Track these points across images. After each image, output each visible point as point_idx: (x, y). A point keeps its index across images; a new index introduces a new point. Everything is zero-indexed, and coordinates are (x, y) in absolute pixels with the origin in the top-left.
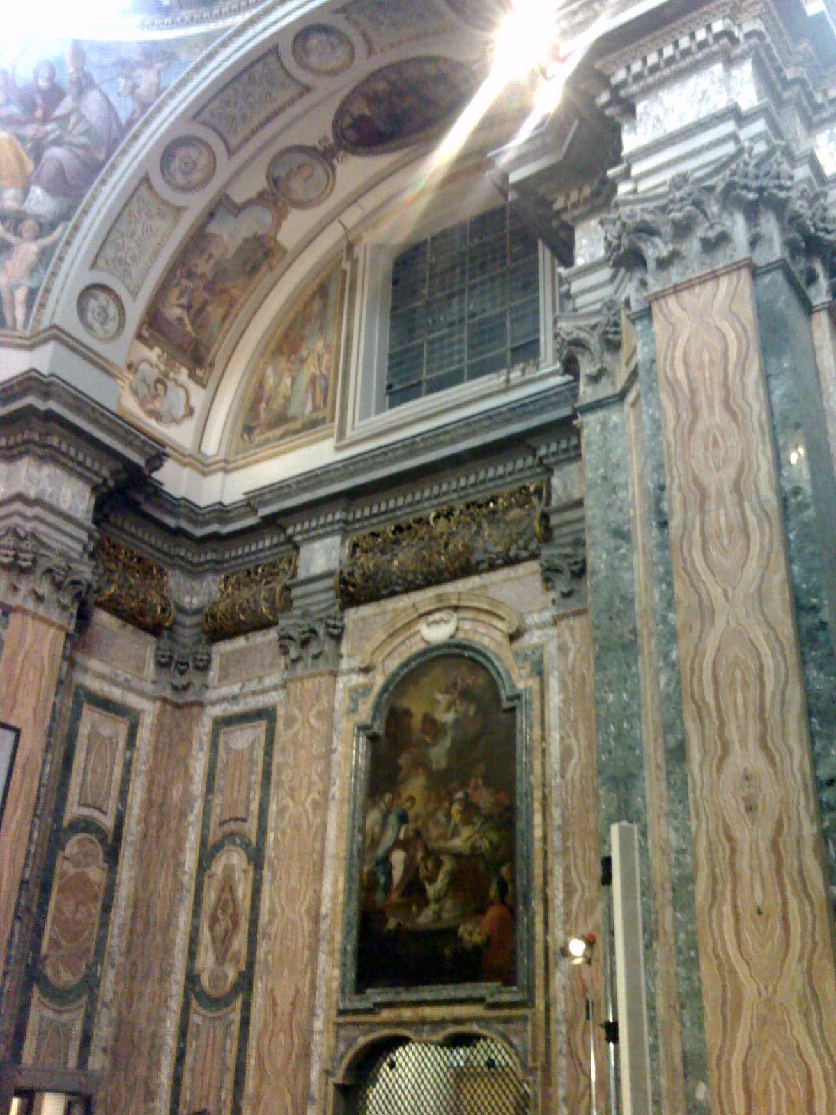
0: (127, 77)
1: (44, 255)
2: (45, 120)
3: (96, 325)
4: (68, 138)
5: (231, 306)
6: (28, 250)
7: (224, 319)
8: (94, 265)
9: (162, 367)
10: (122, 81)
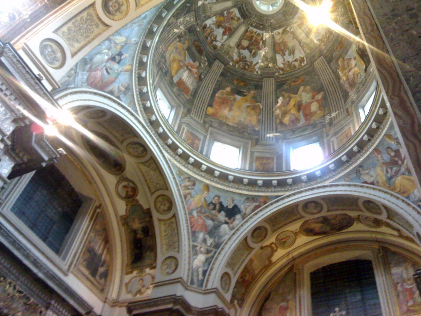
2: (403, 162)
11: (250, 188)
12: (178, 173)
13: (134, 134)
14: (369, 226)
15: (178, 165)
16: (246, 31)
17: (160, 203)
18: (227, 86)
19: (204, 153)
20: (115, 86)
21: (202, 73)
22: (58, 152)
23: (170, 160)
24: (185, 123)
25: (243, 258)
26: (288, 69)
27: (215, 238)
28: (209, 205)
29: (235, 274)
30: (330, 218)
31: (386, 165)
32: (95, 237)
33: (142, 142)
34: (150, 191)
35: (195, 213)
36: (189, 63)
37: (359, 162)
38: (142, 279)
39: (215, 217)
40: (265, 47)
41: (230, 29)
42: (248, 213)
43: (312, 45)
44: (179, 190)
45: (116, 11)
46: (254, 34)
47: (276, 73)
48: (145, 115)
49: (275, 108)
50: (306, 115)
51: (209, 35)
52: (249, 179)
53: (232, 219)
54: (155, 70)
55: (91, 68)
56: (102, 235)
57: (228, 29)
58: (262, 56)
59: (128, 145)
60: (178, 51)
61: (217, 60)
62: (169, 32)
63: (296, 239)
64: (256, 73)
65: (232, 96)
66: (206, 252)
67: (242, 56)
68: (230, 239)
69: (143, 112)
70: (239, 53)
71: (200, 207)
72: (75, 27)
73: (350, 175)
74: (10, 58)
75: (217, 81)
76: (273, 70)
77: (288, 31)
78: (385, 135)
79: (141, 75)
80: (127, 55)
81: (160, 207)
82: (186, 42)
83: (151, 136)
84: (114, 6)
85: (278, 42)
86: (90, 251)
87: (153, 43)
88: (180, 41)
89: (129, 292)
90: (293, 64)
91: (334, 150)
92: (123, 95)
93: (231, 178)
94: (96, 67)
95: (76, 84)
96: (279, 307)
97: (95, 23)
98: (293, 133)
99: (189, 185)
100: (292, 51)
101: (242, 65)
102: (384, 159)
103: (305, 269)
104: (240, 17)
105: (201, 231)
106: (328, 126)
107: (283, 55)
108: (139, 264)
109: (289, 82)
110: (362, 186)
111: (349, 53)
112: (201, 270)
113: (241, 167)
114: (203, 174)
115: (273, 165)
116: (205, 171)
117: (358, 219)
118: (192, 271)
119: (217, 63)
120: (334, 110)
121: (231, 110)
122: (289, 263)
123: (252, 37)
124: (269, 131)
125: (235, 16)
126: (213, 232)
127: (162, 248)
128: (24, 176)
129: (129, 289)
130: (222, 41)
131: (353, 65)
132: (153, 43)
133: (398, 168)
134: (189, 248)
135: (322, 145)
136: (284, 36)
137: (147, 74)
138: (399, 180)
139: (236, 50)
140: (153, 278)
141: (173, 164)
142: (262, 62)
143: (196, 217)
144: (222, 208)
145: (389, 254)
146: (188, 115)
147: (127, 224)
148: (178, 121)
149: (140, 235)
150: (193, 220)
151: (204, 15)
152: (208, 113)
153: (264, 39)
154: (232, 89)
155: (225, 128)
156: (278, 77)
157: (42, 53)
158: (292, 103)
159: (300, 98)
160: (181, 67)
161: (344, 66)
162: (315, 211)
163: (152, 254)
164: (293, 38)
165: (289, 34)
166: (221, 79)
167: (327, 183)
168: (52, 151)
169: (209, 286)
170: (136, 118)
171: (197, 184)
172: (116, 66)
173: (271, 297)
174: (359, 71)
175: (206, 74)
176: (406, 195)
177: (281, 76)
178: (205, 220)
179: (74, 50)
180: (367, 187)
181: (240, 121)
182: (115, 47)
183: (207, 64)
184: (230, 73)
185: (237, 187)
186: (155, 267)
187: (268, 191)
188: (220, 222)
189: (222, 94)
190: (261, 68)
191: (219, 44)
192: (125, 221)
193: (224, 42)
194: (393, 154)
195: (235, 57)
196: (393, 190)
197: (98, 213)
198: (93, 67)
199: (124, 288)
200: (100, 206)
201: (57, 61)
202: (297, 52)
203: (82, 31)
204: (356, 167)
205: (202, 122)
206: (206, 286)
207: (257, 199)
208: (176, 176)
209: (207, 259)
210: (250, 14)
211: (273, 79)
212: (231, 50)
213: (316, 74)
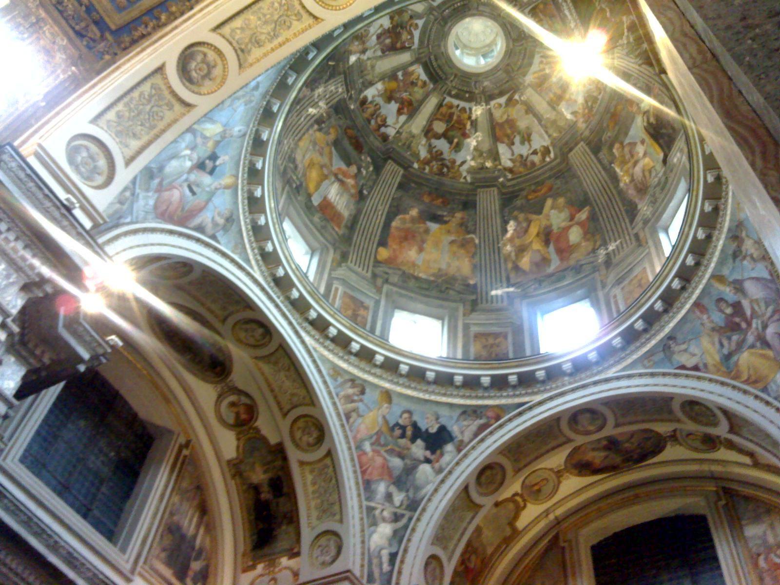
0: (744, 258)
2: (749, 324)
10: (745, 262)
11: (468, 392)
12: (331, 372)
13: (247, 304)
14: (696, 450)
15: (331, 357)
16: (440, 106)
17: (300, 431)
18: (413, 207)
19: (378, 332)
20: (206, 217)
21: (363, 185)
22: (107, 342)
23: (315, 349)
24: (337, 279)
25: (464, 525)
26: (521, 169)
27: (407, 491)
28: (392, 429)
29: (450, 559)
30: (620, 439)
31: (718, 331)
32: (181, 504)
33: (259, 318)
34: (281, 409)
35: (367, 447)
36: (340, 169)
37: (667, 330)
38: (274, 579)
39: (405, 452)
40: (476, 131)
41: (410, 103)
42: (466, 439)
43: (562, 123)
44: (334, 404)
45: (204, 77)
46: (453, 110)
47: (499, 177)
48: (264, 268)
49: (501, 242)
50: (560, 252)
51: (372, 115)
52: (465, 376)
53: (438, 452)
54: (279, 185)
55: (160, 184)
56: (194, 498)
57: (406, 103)
58: (472, 148)
59: (235, 324)
60: (317, 148)
61: (390, 161)
62: (299, 114)
63: (559, 483)
64: (462, 180)
65: (422, 225)
66: (393, 517)
67: (434, 150)
68: (436, 490)
69: (261, 263)
70: (430, 145)
71: (377, 433)
72: (130, 110)
73: (652, 356)
74: (13, 172)
75: (393, 199)
77: (517, 101)
78: (713, 276)
79: (253, 193)
80: (226, 158)
81: (300, 439)
82: (332, 131)
83: (277, 306)
84: (200, 69)
85: (500, 121)
86: (172, 530)
87: (272, 135)
88: (320, 130)
90: (529, 159)
91: (618, 311)
92: (221, 232)
93: (430, 375)
94: (170, 183)
95: (135, 214)
97: (166, 101)
98: (540, 285)
99: (354, 394)
100: (526, 136)
101: (435, 167)
102: (712, 322)
103: (582, 540)
104: (428, 81)
105: (382, 479)
106: (603, 268)
108: (266, 550)
109: (524, 193)
110: (676, 375)
111: (632, 132)
112: (385, 554)
113: (448, 353)
114: (378, 371)
115: (507, 348)
116: (382, 366)
117: (674, 437)
118: (369, 557)
119: (390, 166)
120: (612, 238)
121: (421, 250)
122: (551, 529)
124: (494, 284)
125: (418, 79)
126: (403, 480)
127: (309, 516)
128: (44, 392)
130: (398, 126)
131: (641, 155)
132: (272, 135)
133: (742, 337)
134: (361, 513)
135: (596, 304)
136: (510, 109)
137: (266, 191)
138: (745, 358)
139: (424, 141)
140: (296, 574)
141: (322, 356)
142: (473, 159)
143: (370, 454)
144: (417, 433)
145: (738, 501)
146: (343, 264)
148: (326, 276)
151: (361, 81)
152: (379, 258)
153: (474, 117)
155: (412, 283)
156: (503, 185)
157: (71, 161)
158: (534, 230)
159: (548, 220)
160: (326, 177)
161: (623, 156)
162: (592, 428)
163: (291, 529)
165: (519, 106)
166: (399, 194)
167: (610, 373)
168: (97, 342)
170: (249, 274)
171: (368, 390)
172: (207, 180)
174: (652, 164)
175: (372, 188)
176: (761, 385)
177: (509, 184)
178: (388, 457)
179: (129, 153)
180: (687, 376)
181: (440, 270)
182: (204, 144)
183: (371, 169)
184: (416, 183)
185: (443, 392)
186: (298, 554)
187: (501, 396)
188: (415, 460)
189: (404, 221)
190: (470, 171)
191: (391, 132)
192: (236, 469)
193: (401, 127)
194: (729, 311)
195: (423, 154)
196: (736, 377)
197: (185, 457)
198: (165, 183)
200: (187, 445)
201: (99, 174)
202: (535, 137)
203: (142, 117)
204: (661, 340)
205: (369, 275)
208: (328, 378)
209: (395, 532)
210: (445, 73)
211: (495, 189)
213: (575, 176)
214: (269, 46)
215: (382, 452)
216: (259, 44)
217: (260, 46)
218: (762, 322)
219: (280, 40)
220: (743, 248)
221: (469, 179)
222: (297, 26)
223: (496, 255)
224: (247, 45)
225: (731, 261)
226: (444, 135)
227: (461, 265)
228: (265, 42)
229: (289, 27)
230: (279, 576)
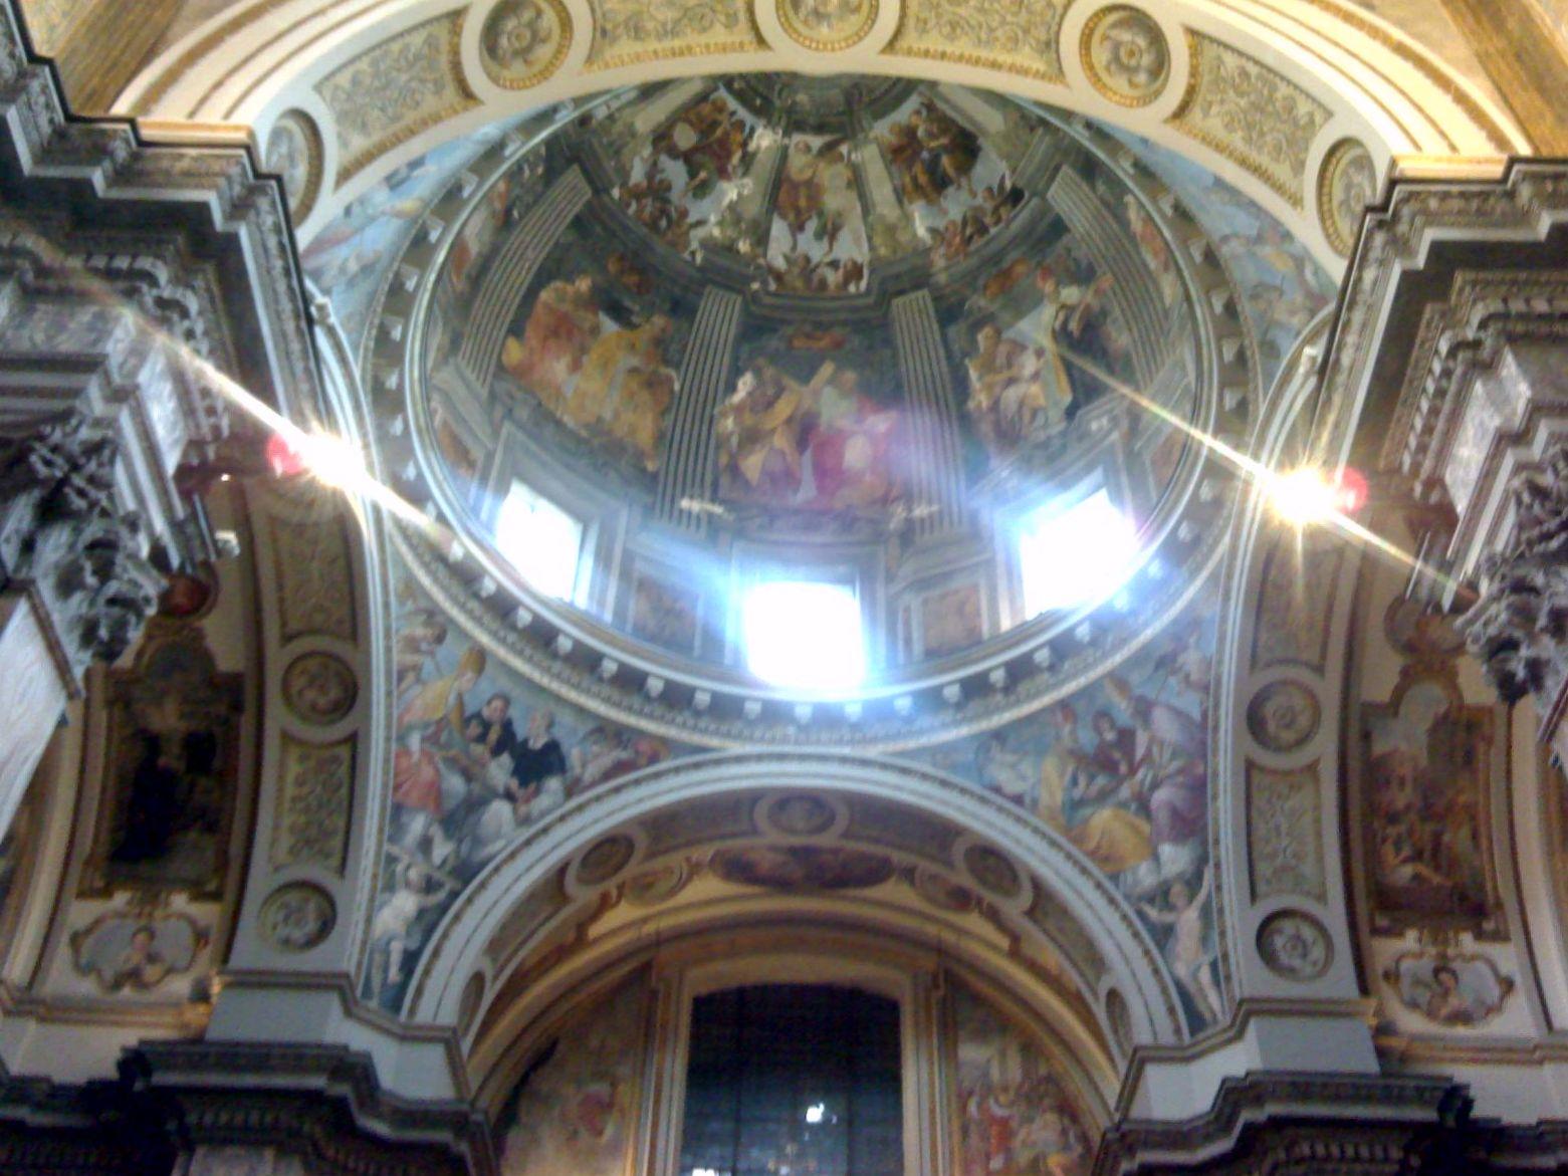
0: (1174, 672)
1: (1206, 913)
2: (1133, 771)
3: (1297, 963)
4: (1162, 773)
5: (1473, 818)
6: (1189, 920)
7: (1475, 836)
8: (1254, 896)
9: (1432, 951)
10: (1173, 681)
11: (616, 695)
14: (931, 900)
22: (215, 542)
27: (460, 841)
28: (466, 722)
29: (496, 977)
34: (284, 624)
35: (415, 741)
40: (745, 174)
45: (517, 53)
47: (753, 279)
53: (532, 786)
58: (726, 202)
61: (576, 167)
63: (690, 878)
64: (686, 255)
65: (590, 316)
72: (376, 75)
74: (261, 232)
75: (557, 244)
76: (748, 265)
77: (841, 156)
81: (300, 692)
84: (518, 37)
89: (83, 969)
90: (819, 271)
96: (580, 1097)
99: (424, 638)
100: (829, 226)
101: (648, 210)
105: (422, 808)
107: (798, 227)
108: (146, 869)
109: (789, 330)
110: (983, 800)
117: (909, 874)
119: (573, 176)
123: (715, 124)
126: (458, 819)
129: (83, 961)
136: (822, 165)
138: (1103, 819)
139: (647, 151)
141: (397, 553)
142: (720, 223)
143: (416, 756)
144: (507, 741)
145: (962, 1001)
147: (127, 705)
149: (171, 759)
150: (404, 762)
153: (752, 146)
154: (595, 289)
155: (549, 431)
156: (755, 296)
158: (783, 408)
161: (992, 356)
163: (209, 844)
164: (849, 185)
165: (840, 168)
166: (571, 237)
169: (424, 1015)
171: (450, 637)
173: (557, 1056)
174: (1042, 401)
175: (529, 208)
177: (767, 300)
180: (1000, 809)
181: (599, 419)
183: (540, 170)
184: (605, 228)
189: (562, 299)
190: (708, 244)
193: (619, 109)
195: (637, 175)
199: (62, 952)
202: (844, 236)
203: (388, 93)
205: (484, 393)
206: (412, 1012)
207: (629, 740)
208: (393, 599)
209: (422, 912)
212: (631, 145)
213: (888, 342)
214: (653, 45)
215: (437, 759)
216: (637, 32)
217: (637, 37)
218: (1155, 777)
219: (677, 43)
220: (1181, 660)
221: (699, 258)
222: (719, 34)
223: (705, 428)
224: (616, 27)
225: (1150, 667)
226: (688, 157)
227: (642, 426)
228: (648, 35)
229: (704, 30)
230: (159, 925)
